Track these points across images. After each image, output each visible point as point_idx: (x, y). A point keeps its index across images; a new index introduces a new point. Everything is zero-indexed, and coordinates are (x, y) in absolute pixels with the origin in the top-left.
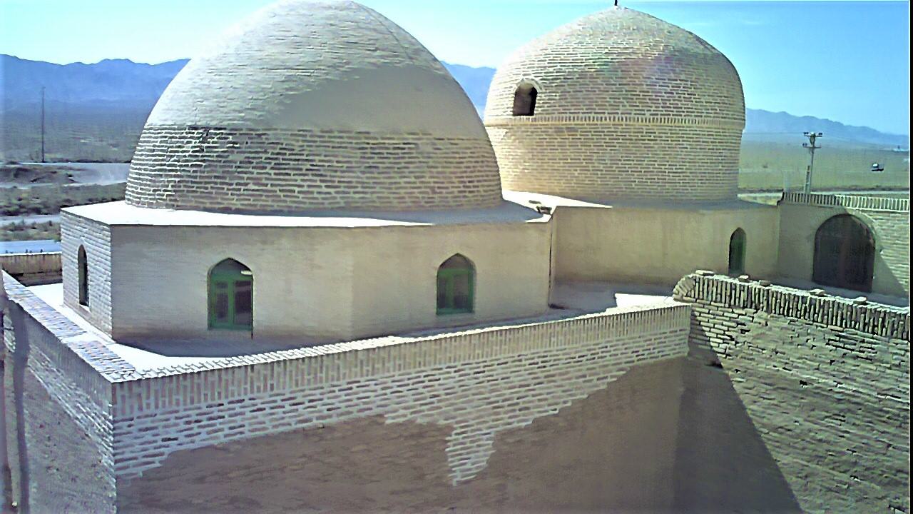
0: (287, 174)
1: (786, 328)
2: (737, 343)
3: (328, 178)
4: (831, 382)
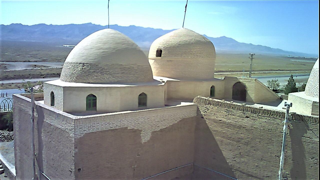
0: (104, 75)
2: (207, 112)
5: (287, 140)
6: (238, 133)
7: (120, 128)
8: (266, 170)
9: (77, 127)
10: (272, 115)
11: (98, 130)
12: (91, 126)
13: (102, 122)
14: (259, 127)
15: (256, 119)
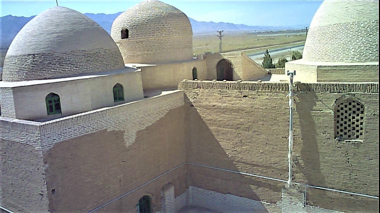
1: (208, 92)
3: (76, 65)
4: (220, 104)
5: (294, 117)
6: (237, 118)
7: (97, 132)
8: (273, 156)
9: (44, 137)
10: (274, 89)
11: (71, 138)
12: (61, 133)
13: (74, 126)
14: (260, 107)
15: (256, 96)
